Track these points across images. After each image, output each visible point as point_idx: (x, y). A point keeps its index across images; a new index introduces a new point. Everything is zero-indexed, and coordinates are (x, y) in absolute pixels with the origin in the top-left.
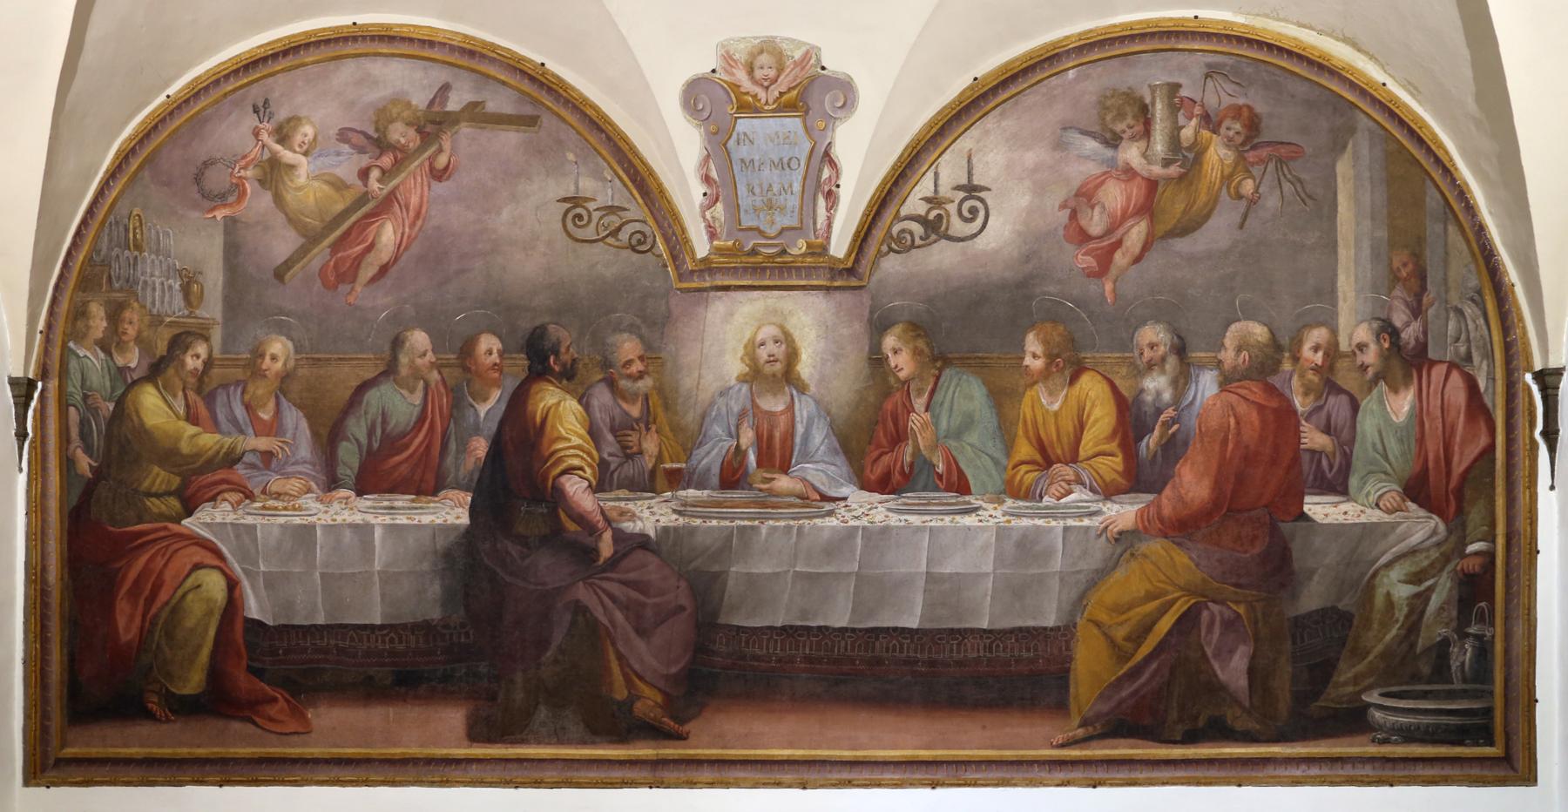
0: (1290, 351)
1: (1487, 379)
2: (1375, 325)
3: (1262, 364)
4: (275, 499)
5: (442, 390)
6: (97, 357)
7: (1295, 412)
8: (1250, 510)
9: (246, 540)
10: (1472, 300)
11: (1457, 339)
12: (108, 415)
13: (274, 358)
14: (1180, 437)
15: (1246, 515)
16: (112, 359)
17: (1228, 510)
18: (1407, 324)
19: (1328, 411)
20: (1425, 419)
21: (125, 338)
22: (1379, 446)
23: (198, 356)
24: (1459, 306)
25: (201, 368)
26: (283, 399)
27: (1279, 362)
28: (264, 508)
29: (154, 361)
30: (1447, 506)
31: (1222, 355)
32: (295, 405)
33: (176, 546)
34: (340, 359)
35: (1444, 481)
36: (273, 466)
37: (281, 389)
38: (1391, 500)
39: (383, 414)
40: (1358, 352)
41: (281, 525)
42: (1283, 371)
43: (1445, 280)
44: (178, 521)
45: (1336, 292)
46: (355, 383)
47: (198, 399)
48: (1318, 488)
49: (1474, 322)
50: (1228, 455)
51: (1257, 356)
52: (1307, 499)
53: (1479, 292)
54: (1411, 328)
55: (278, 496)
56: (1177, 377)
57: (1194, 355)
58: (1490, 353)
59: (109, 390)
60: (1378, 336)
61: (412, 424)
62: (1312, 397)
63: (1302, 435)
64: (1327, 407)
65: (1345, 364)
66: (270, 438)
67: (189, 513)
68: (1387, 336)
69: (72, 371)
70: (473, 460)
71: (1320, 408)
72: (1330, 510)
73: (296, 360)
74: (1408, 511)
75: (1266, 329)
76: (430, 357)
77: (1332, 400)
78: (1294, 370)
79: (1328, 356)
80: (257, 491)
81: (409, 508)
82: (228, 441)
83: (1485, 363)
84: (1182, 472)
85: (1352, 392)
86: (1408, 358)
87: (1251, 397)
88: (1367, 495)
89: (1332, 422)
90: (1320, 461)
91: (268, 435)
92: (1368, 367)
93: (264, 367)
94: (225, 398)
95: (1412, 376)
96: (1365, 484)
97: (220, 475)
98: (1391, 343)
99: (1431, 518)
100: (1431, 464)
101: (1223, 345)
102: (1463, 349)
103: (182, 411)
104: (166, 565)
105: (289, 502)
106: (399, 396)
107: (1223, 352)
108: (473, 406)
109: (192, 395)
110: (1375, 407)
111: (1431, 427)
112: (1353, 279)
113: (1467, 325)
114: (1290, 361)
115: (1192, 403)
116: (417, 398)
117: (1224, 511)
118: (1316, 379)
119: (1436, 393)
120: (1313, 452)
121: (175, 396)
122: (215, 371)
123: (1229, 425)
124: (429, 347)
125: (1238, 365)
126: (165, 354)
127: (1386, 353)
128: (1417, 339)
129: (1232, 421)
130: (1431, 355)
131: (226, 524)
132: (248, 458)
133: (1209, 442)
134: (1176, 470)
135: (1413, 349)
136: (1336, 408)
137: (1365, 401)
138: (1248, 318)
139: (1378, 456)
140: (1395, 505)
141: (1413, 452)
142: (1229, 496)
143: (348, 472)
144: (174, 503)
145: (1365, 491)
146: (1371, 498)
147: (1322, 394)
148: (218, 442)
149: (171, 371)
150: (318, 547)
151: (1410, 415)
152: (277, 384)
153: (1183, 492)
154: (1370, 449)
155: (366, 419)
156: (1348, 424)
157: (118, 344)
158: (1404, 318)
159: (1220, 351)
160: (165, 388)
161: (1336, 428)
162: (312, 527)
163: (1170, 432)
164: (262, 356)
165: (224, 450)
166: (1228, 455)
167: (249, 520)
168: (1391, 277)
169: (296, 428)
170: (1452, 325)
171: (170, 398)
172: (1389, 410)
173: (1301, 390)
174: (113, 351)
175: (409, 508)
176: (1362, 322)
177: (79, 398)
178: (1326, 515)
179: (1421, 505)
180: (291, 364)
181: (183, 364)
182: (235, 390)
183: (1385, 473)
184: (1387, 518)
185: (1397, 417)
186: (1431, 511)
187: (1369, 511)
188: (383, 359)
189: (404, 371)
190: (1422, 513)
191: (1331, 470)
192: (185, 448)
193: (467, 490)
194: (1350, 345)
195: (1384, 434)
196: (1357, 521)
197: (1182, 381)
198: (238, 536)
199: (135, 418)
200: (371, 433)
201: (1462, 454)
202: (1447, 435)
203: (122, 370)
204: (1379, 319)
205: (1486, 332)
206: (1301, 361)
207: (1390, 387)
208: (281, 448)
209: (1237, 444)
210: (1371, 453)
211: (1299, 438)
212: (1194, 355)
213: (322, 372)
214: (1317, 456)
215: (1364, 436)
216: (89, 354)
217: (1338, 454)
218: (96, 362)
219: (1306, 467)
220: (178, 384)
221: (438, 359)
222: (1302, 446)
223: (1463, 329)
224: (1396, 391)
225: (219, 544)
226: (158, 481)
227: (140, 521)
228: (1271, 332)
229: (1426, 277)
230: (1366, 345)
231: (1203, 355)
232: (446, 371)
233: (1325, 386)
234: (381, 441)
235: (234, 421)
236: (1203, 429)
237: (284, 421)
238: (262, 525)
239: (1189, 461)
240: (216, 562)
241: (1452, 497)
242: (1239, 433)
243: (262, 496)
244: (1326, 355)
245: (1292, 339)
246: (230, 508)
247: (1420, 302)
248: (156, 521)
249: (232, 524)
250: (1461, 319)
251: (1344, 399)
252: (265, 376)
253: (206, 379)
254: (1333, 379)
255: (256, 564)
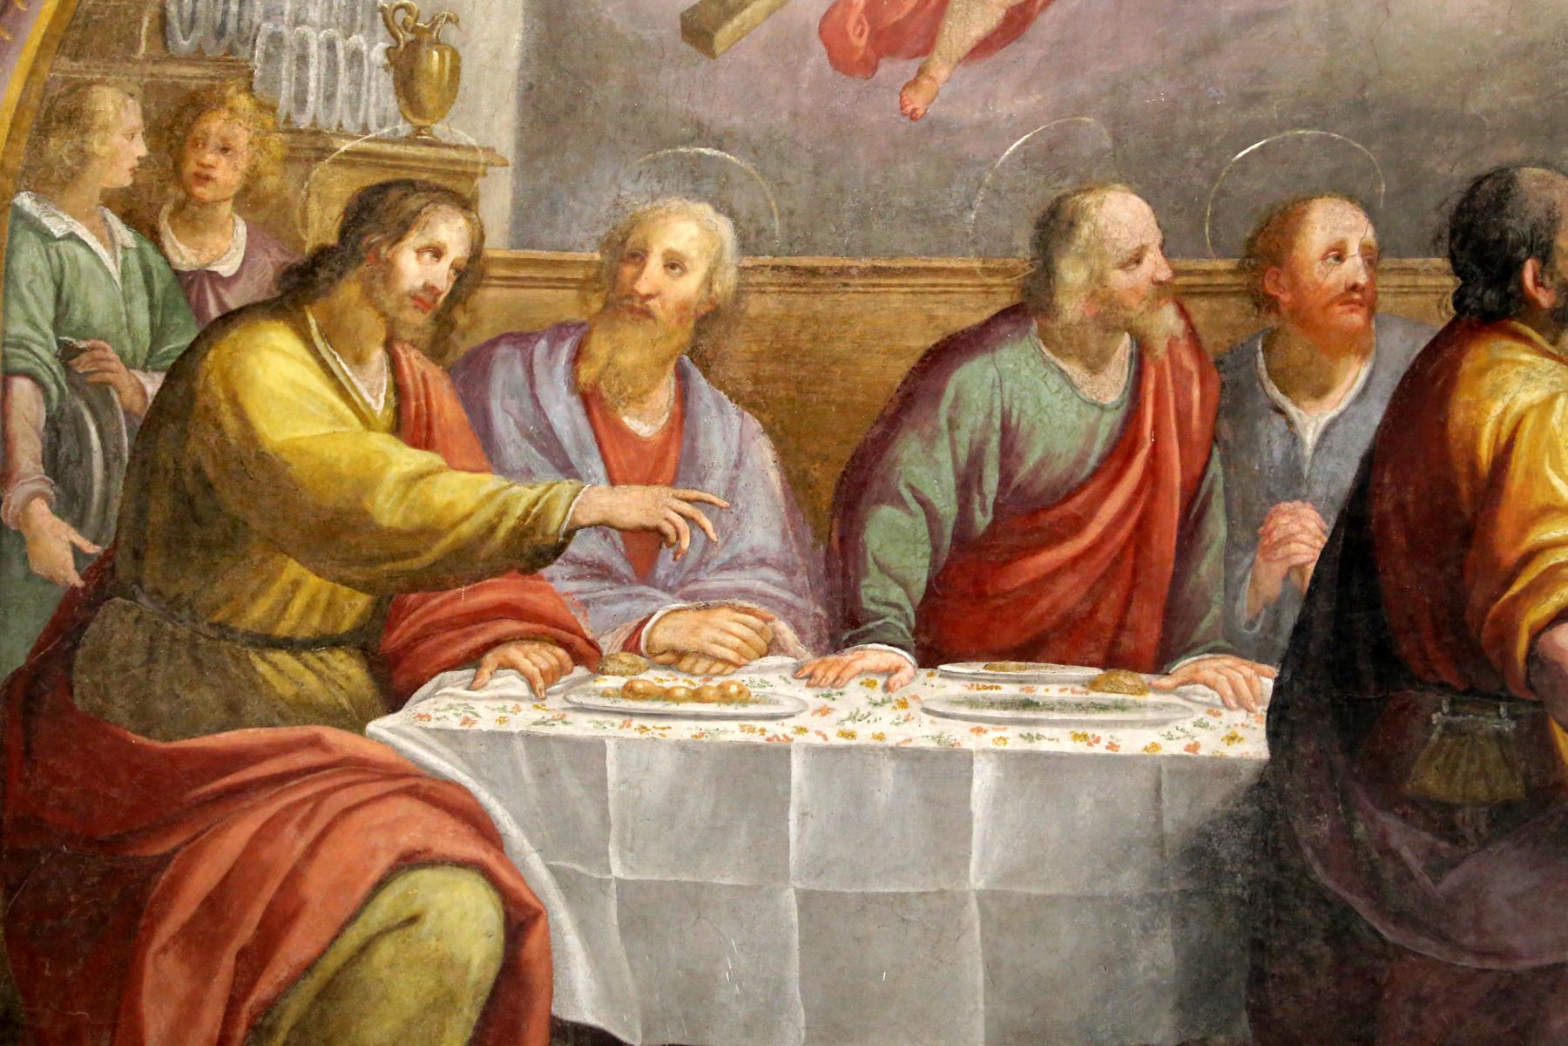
4: (667, 666)
5: (1189, 362)
6: (110, 240)
9: (571, 784)
12: (140, 407)
13: (674, 263)
16: (159, 248)
21: (204, 192)
23: (438, 253)
25: (444, 283)
26: (699, 380)
28: (629, 691)
29: (297, 259)
32: (735, 397)
33: (345, 798)
34: (877, 271)
36: (661, 572)
37: (694, 352)
39: (1005, 428)
41: (682, 747)
44: (356, 721)
46: (921, 341)
47: (434, 372)
55: (676, 658)
59: (145, 338)
61: (1092, 462)
66: (655, 490)
67: (395, 700)
69: (24, 278)
70: (1279, 569)
73: (743, 270)
76: (1155, 266)
80: (609, 643)
81: (1079, 707)
82: (523, 496)
91: (649, 481)
93: (643, 287)
94: (519, 371)
97: (493, 593)
103: (380, 404)
104: (311, 852)
105: (708, 675)
106: (1054, 381)
108: (1280, 411)
109: (415, 362)
116: (1111, 386)
121: (359, 360)
122: (491, 298)
124: (1153, 237)
126: (332, 241)
131: (509, 736)
132: (585, 547)
143: (896, 594)
144: (348, 670)
148: (490, 497)
149: (349, 291)
150: (793, 814)
152: (682, 337)
155: (953, 443)
157: (180, 207)
160: (327, 337)
162: (774, 757)
164: (639, 257)
165: (509, 522)
167: (582, 727)
169: (738, 465)
171: (342, 366)
174: (164, 226)
175: (1079, 707)
177: (47, 357)
180: (728, 280)
181: (388, 271)
182: (551, 351)
188: (1008, 272)
189: (1071, 307)
192: (387, 510)
193: (1262, 657)
198: (544, 774)
199: (230, 423)
200: (967, 483)
203: (191, 283)
208: (689, 519)
213: (821, 305)
216: (82, 231)
218: (105, 255)
220: (370, 325)
221: (1177, 273)
225: (485, 796)
226: (298, 604)
227: (234, 716)
232: (1200, 308)
234: (997, 506)
235: (546, 440)
237: (701, 444)
238: (623, 744)
240: (473, 849)
243: (627, 658)
246: (521, 688)
248: (285, 719)
249: (528, 737)
252: (647, 314)
253: (462, 319)
255: (598, 855)
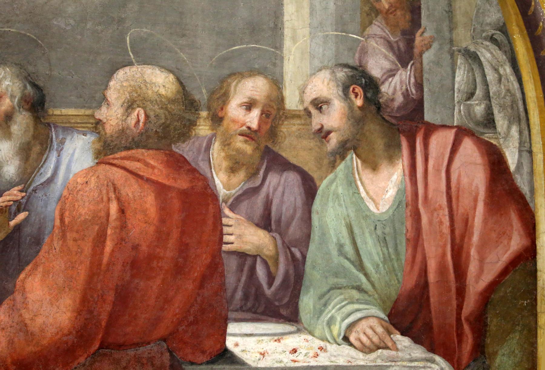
0: (209, 109)
1: (520, 151)
2: (341, 74)
3: (165, 127)
7: (214, 197)
8: (137, 345)
10: (492, 39)
11: (471, 95)
14: (27, 230)
15: (131, 352)
17: (101, 347)
18: (391, 73)
19: (268, 196)
20: (420, 206)
22: (349, 249)
24: (472, 49)
27: (193, 124)
30: (460, 341)
31: (102, 113)
35: (454, 303)
38: (370, 332)
40: (314, 111)
42: (197, 137)
43: (450, 12)
45: (282, 28)
48: (249, 310)
49: (496, 70)
50: (105, 259)
51: (157, 116)
52: (232, 328)
53: (503, 29)
54: (397, 78)
56: (29, 143)
57: (57, 112)
58: (523, 114)
60: (345, 89)
62: (241, 175)
63: (226, 230)
64: (264, 189)
65: (294, 128)
68: (359, 90)
71: (256, 190)
72: (269, 345)
74: (397, 350)
75: (171, 77)
77: (273, 179)
78: (214, 135)
79: (268, 116)
83: (514, 130)
84: (28, 285)
85: (306, 169)
86: (394, 121)
87: (146, 173)
88: (330, 322)
89: (273, 214)
90: (253, 269)
92: (329, 132)
95: (399, 146)
96: (325, 305)
98: (366, 98)
99: (433, 361)
100: (432, 277)
101: (104, 98)
102: (479, 109)
107: (104, 109)
110: (340, 190)
111: (430, 222)
112: (306, 11)
113: (484, 76)
114: (209, 123)
115: (51, 180)
117: (96, 345)
118: (248, 149)
119: (438, 171)
120: (242, 255)
123: (108, 215)
125: (128, 128)
127: (358, 113)
128: (406, 95)
129: (114, 208)
130: (428, 117)
133: (75, 240)
134: (18, 282)
135: (399, 108)
136: (280, 189)
137: (325, 182)
138: (145, 62)
139: (347, 264)
140: (375, 339)
141: (403, 257)
142: (103, 324)
145: (326, 317)
146: (336, 329)
147: (258, 170)
151: (398, 204)
153: (27, 316)
154: (335, 253)
156: (299, 214)
158: (387, 65)
159: (99, 107)
161: (279, 221)
163: (12, 223)
166: (105, 259)
168: (367, 8)
170: (461, 76)
172: (363, 194)
173: (225, 164)
176: (320, 70)
178: (263, 354)
179: (417, 340)
183: (359, 289)
184: (361, 359)
185: (376, 205)
186: (432, 349)
187: (332, 348)
190: (419, 352)
191: (270, 284)
194: (302, 101)
195: (356, 230)
196: (313, 363)
197: (37, 149)
201: (482, 260)
202: (457, 232)
204: (346, 66)
205: (516, 85)
206: (225, 123)
207: (364, 161)
209: (121, 241)
210: (337, 259)
211: (222, 234)
212: (57, 112)
214: (249, 262)
215: (324, 234)
217: (282, 259)
219: (230, 279)
222: (225, 247)
223: (479, 80)
224: (374, 167)
228: (178, 79)
229: (419, 8)
230: (327, 102)
231: (71, 111)
233: (262, 158)
236: (67, 220)
239: (40, 269)
241: (466, 328)
242: (123, 226)
244: (265, 114)
245: (212, 93)
247: (410, 43)
250: (475, 67)
251: (292, 178)
254: (276, 149)
